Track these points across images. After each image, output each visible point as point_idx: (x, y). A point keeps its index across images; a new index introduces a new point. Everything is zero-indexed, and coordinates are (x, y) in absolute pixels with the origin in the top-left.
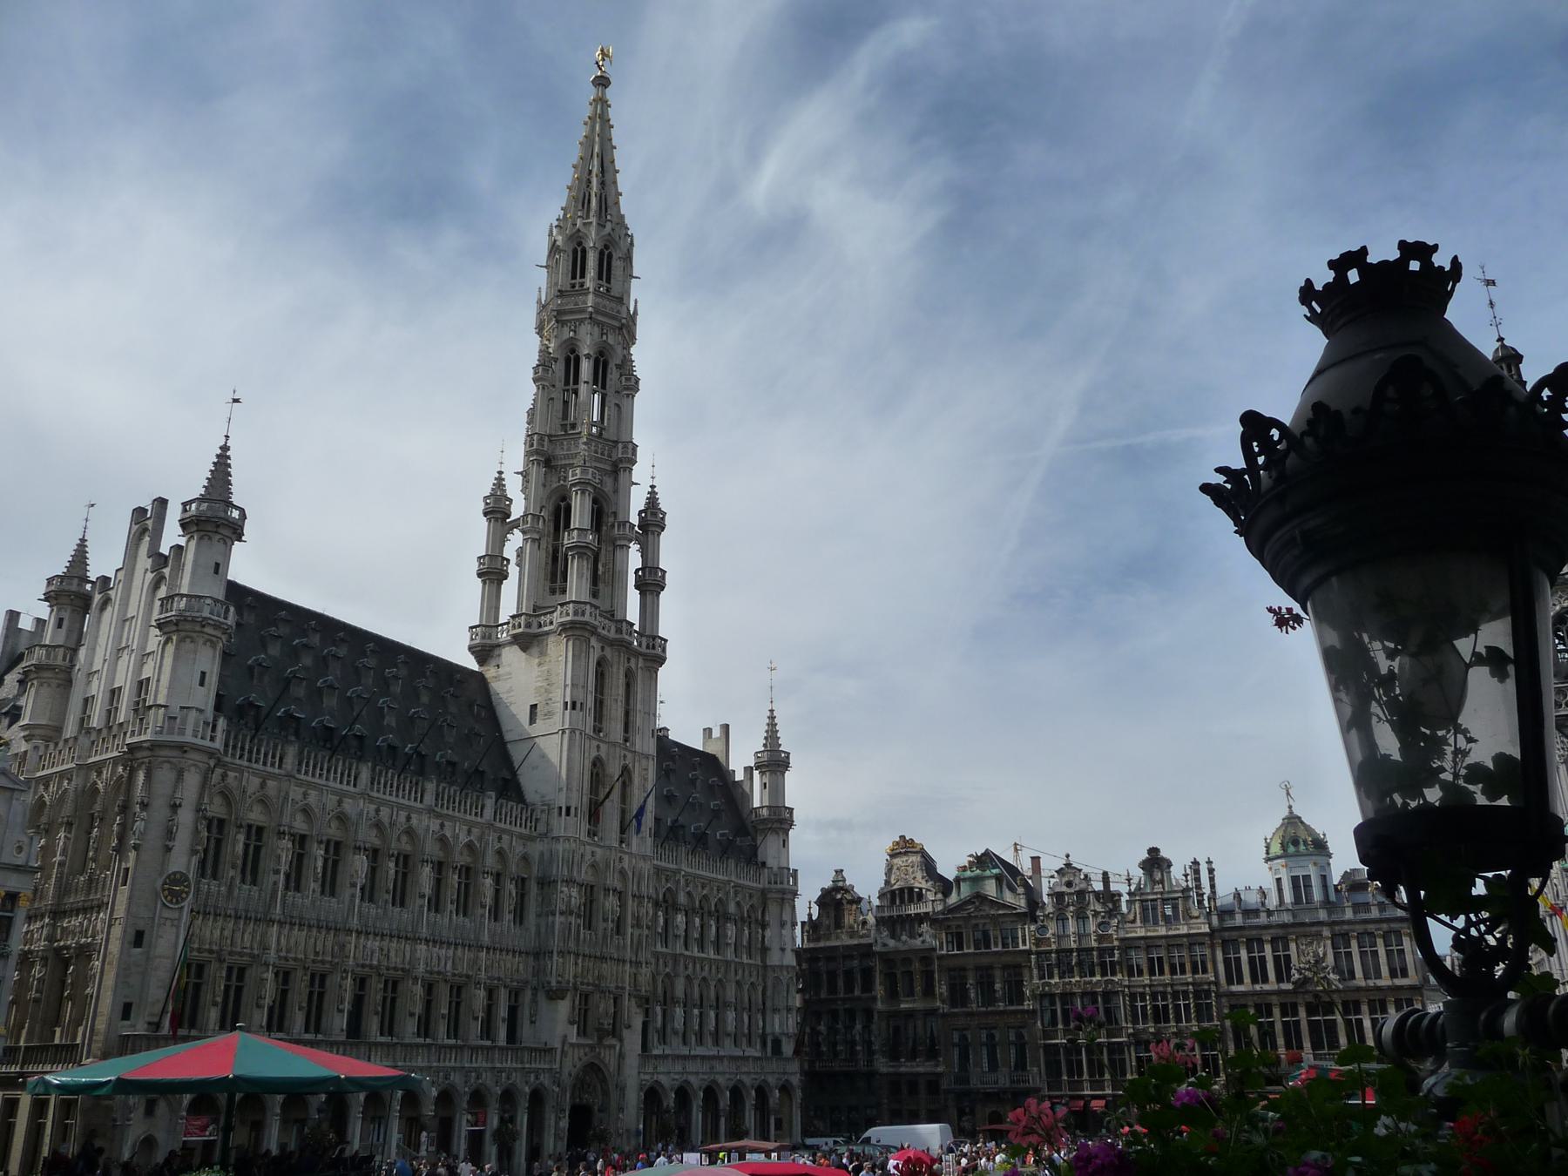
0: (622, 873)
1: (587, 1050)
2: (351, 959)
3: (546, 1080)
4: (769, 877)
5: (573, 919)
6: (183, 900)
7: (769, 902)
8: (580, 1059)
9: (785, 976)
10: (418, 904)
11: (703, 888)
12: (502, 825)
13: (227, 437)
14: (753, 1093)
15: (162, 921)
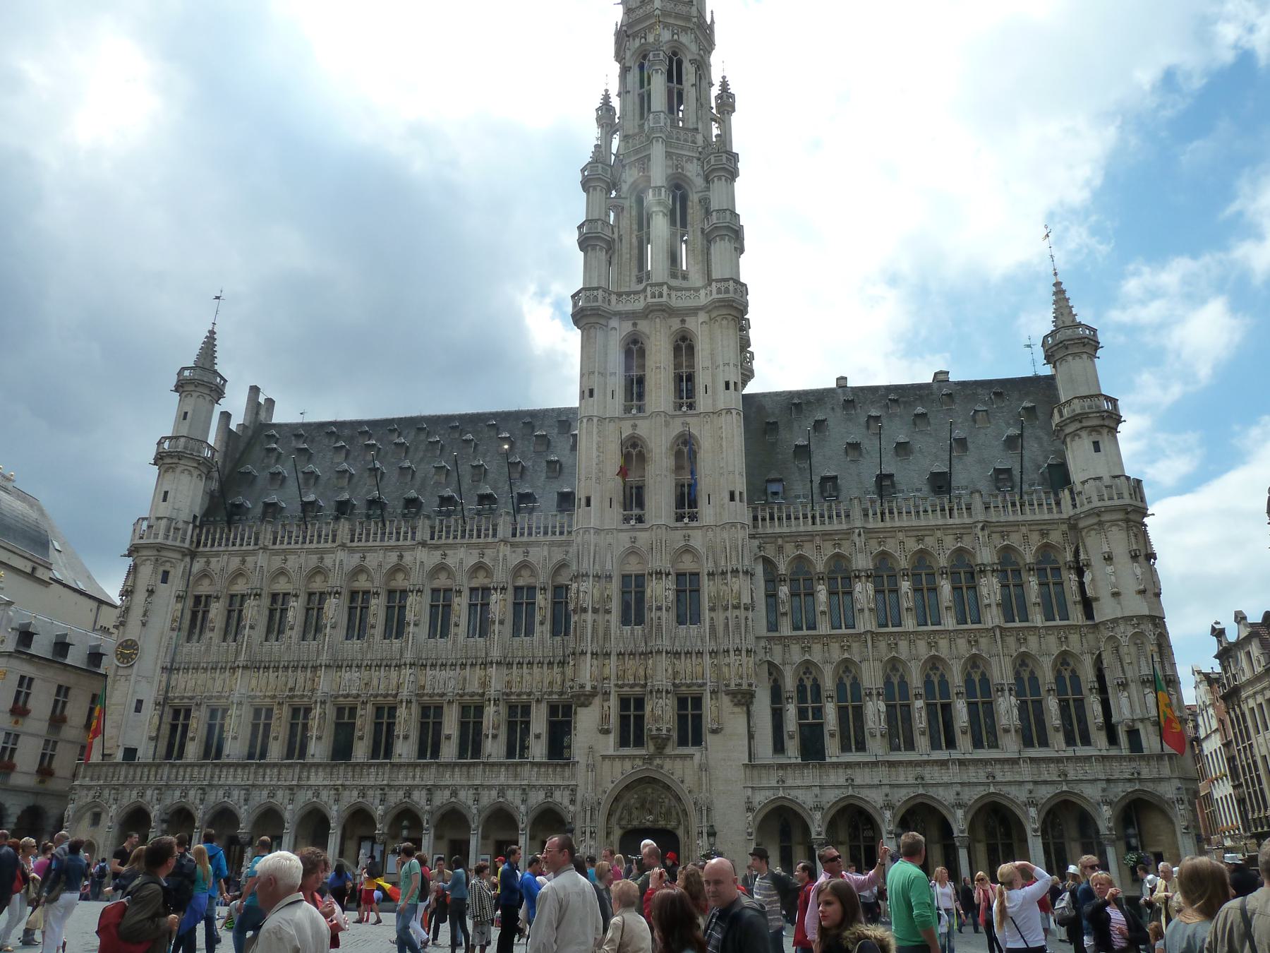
0: (688, 550)
1: (638, 762)
2: (320, 691)
3: (562, 798)
4: (1073, 499)
5: (589, 616)
6: (132, 659)
7: (1084, 534)
8: (623, 774)
9: (1124, 633)
10: (418, 632)
11: (920, 539)
12: (525, 539)
13: (214, 324)
14: (1033, 812)
15: (118, 678)
